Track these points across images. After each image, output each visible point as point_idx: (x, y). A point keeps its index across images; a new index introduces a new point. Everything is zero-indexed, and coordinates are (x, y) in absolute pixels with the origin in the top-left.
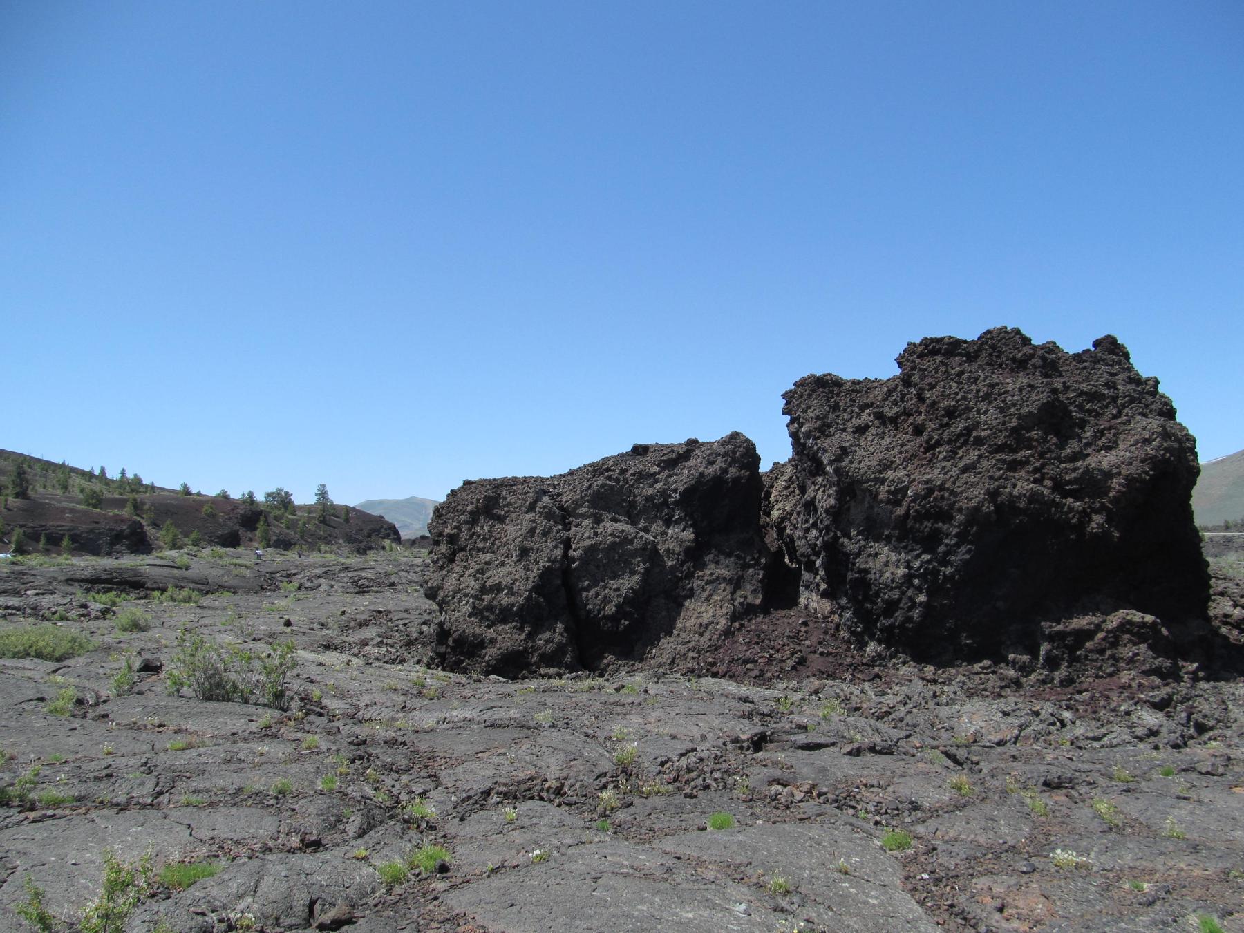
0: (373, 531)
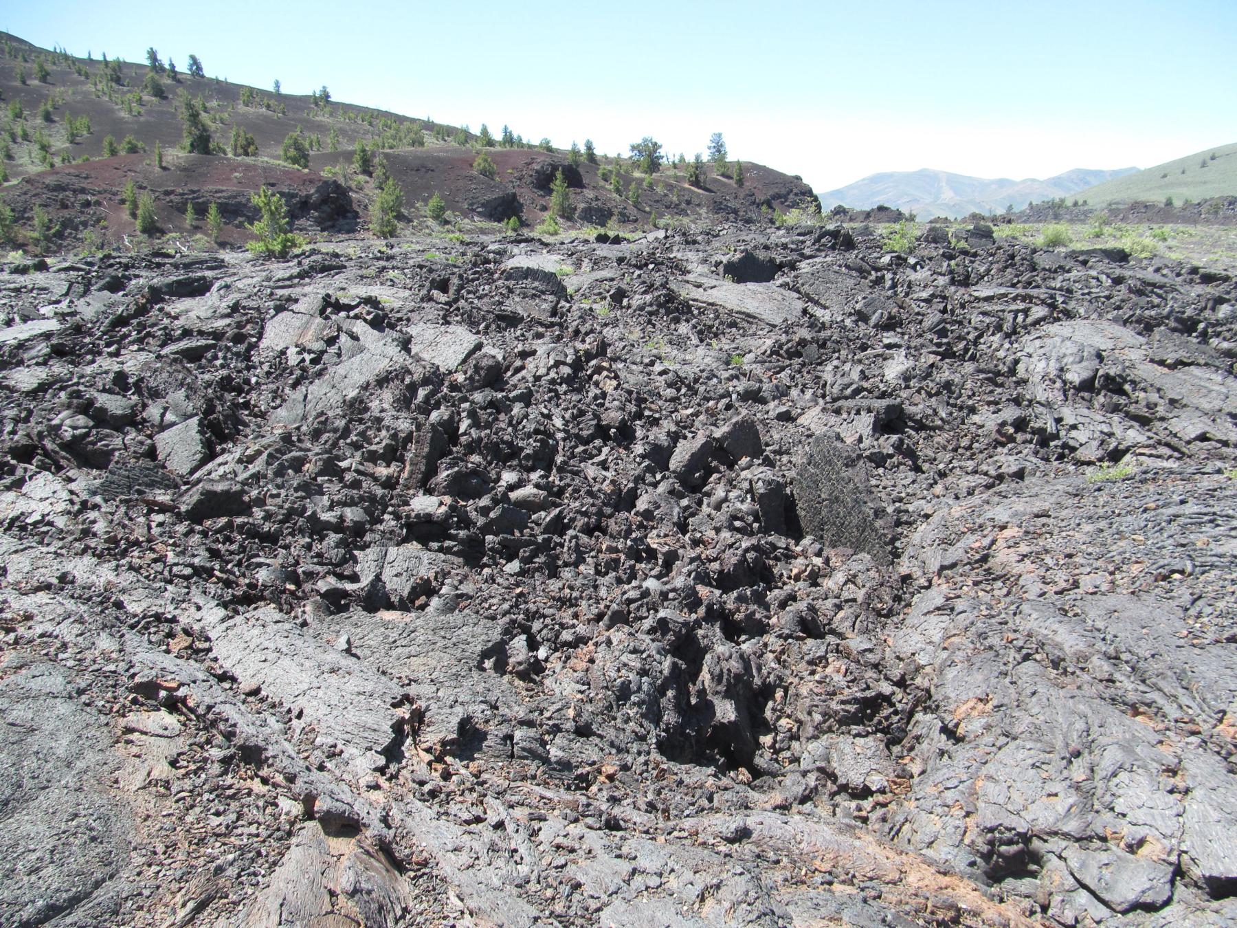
0: (776, 196)
